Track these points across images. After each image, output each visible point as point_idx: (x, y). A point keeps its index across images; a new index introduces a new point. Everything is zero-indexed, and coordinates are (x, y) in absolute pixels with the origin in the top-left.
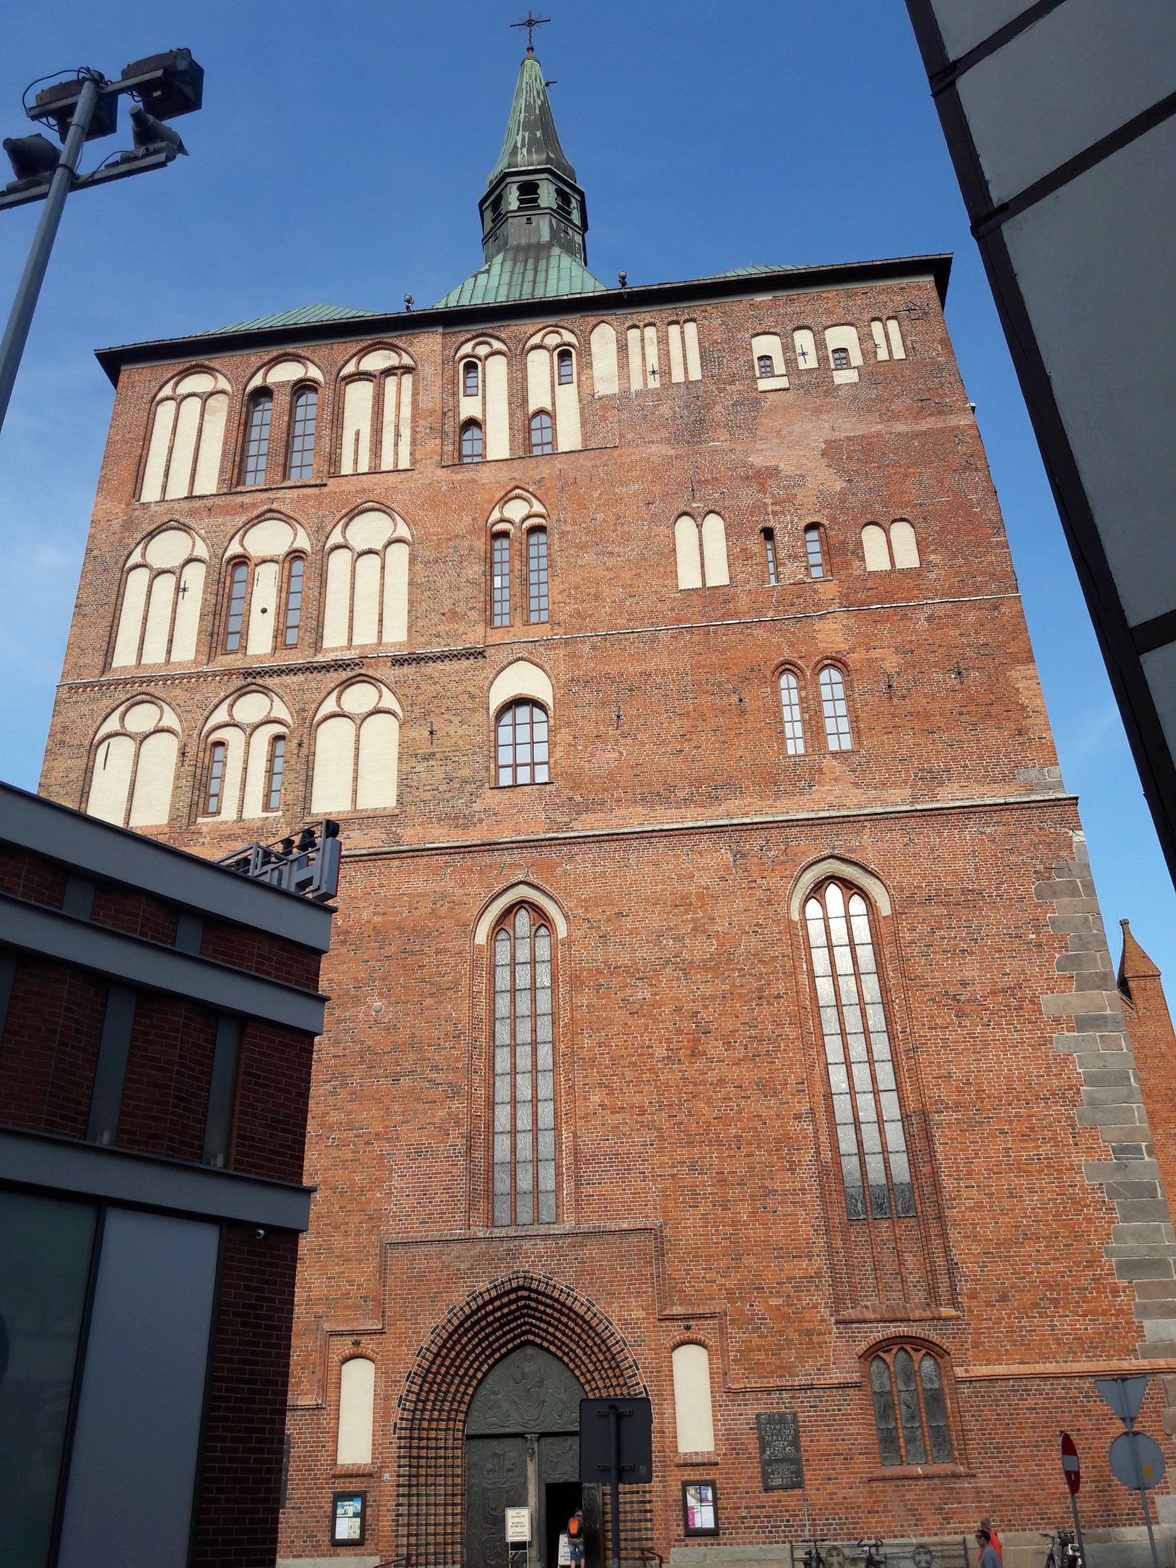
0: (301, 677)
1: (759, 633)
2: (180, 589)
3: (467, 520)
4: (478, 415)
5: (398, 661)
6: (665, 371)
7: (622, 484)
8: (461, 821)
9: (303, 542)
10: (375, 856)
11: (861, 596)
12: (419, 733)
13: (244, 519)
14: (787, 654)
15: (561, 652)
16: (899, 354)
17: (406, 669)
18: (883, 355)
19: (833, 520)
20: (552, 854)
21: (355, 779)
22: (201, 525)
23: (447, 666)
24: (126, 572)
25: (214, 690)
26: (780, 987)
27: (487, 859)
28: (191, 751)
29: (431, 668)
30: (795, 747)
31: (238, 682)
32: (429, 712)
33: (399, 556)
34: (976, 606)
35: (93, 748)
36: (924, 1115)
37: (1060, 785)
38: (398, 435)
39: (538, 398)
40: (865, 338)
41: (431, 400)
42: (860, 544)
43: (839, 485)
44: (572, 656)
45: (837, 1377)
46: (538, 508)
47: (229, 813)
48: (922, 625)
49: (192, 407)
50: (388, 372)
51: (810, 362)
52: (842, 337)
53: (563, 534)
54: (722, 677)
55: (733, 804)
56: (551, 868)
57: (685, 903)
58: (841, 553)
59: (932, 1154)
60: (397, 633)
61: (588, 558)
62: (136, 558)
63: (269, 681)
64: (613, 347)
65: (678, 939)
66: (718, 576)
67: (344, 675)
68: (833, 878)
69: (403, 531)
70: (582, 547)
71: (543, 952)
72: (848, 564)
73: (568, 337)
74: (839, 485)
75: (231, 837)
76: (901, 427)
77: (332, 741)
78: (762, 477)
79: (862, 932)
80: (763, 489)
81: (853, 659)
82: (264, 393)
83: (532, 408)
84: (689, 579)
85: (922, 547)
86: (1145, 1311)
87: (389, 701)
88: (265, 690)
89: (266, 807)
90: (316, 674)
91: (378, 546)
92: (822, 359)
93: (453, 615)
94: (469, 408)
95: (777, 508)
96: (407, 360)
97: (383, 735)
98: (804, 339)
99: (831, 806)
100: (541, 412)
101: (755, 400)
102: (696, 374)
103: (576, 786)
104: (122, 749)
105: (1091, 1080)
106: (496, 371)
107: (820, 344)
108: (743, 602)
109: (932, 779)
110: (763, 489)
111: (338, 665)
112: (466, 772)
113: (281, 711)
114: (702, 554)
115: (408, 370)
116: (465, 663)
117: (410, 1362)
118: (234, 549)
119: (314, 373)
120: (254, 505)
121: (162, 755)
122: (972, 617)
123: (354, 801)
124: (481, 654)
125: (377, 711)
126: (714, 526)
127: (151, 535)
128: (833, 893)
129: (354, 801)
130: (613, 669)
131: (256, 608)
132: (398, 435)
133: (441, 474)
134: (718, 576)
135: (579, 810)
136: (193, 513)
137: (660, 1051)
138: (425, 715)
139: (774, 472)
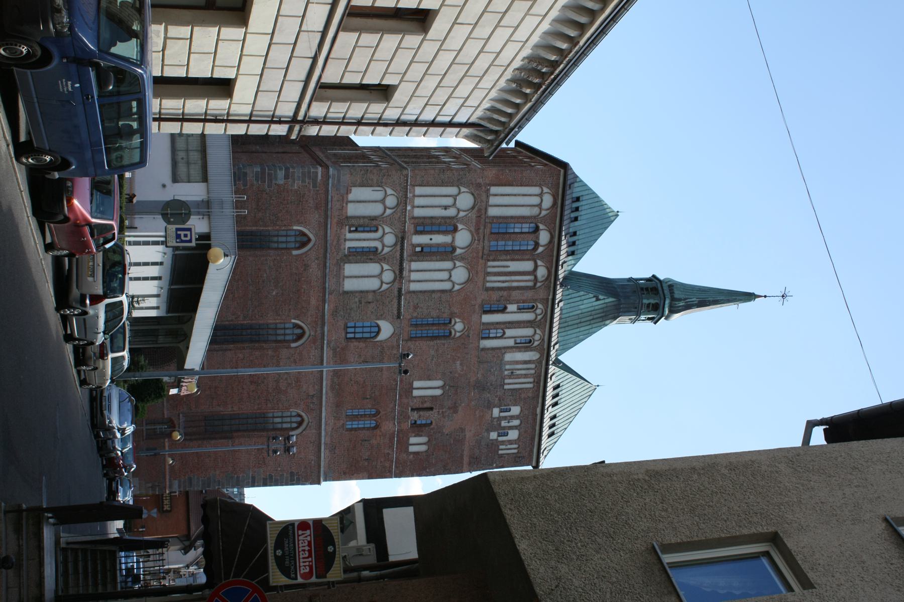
0: (398, 257)
1: (392, 405)
3: (456, 311)
4: (508, 310)
5: (400, 290)
6: (512, 375)
7: (461, 364)
9: (458, 251)
10: (324, 288)
11: (401, 435)
12: (370, 297)
14: (382, 413)
15: (395, 343)
16: (500, 452)
17: (396, 293)
18: (501, 447)
19: (433, 429)
21: (356, 277)
22: (473, 215)
23: (396, 305)
26: (269, 405)
27: (319, 323)
28: (374, 223)
29: (395, 301)
30: (349, 412)
32: (377, 301)
33: (447, 286)
34: (391, 467)
36: (231, 438)
37: (325, 480)
38: (503, 282)
39: (509, 332)
40: (510, 442)
42: (421, 436)
43: (446, 431)
45: (165, 412)
46: (458, 334)
47: (349, 236)
48: (387, 451)
49: (536, 200)
50: (536, 277)
51: (504, 424)
52: (513, 435)
53: (444, 344)
54: (377, 393)
55: (330, 394)
56: (314, 343)
58: (418, 429)
59: (221, 438)
60: (414, 287)
61: (432, 352)
62: (463, 189)
63: (398, 247)
64: (528, 359)
65: (286, 379)
66: (416, 393)
67: (397, 272)
68: (303, 421)
69: (457, 287)
70: (437, 350)
71: (288, 338)
72: (413, 432)
73: (536, 343)
74: (446, 431)
77: (373, 268)
78: (454, 408)
79: (285, 426)
80: (449, 408)
81: (378, 432)
83: (506, 331)
84: (416, 384)
85: (416, 454)
86: (180, 482)
87: (385, 287)
88: (395, 244)
90: (398, 263)
91: (453, 279)
92: (504, 428)
93: (416, 307)
94: (512, 307)
96: (539, 284)
97: (373, 284)
98: (516, 422)
99: (326, 422)
100: (504, 333)
101: (490, 406)
102: (506, 387)
103: (343, 349)
104: (379, 195)
105: (238, 477)
106: (528, 316)
107: (511, 428)
108: (405, 401)
109: (332, 448)
110: (449, 408)
111: (401, 270)
113: (386, 250)
114: (426, 388)
115: (535, 284)
116: (396, 312)
118: (460, 226)
119: (541, 249)
120: (478, 234)
121: (375, 210)
122: (387, 465)
123: (347, 277)
124: (399, 317)
125: (382, 282)
126: (438, 392)
128: (299, 419)
129: (347, 277)
131: (432, 236)
132: (503, 282)
133: (479, 301)
134: (416, 393)
135: (334, 350)
136: (479, 210)
138: (377, 301)
139: (456, 412)
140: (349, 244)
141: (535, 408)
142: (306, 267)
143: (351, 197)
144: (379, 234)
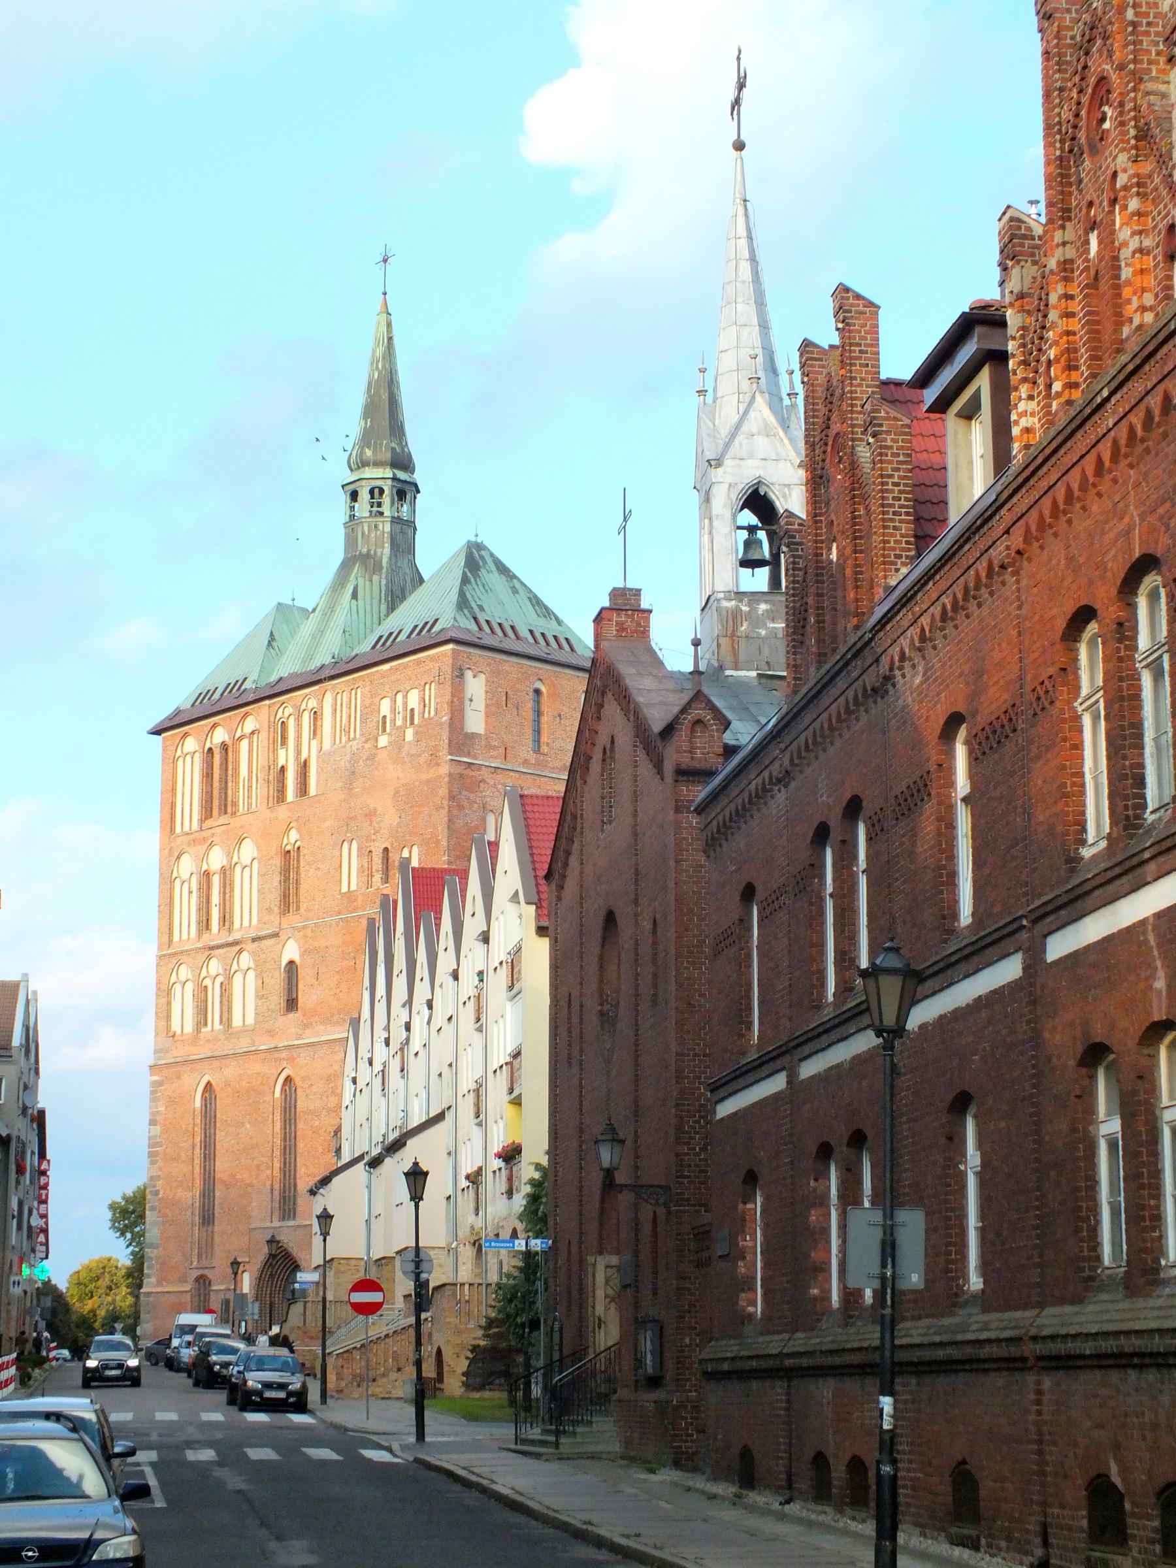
2: (190, 892)
5: (254, 940)
8: (271, 1033)
13: (205, 847)
20: (294, 1053)
24: (172, 882)
25: (202, 957)
27: (276, 1055)
31: (207, 953)
35: (169, 990)
41: (261, 759)
44: (305, 936)
50: (253, 733)
57: (329, 1080)
63: (216, 952)
67: (238, 948)
75: (208, 1041)
76: (424, 777)
82: (210, 749)
84: (344, 889)
89: (221, 1022)
92: (405, 719)
95: (374, 837)
108: (360, 899)
111: (236, 943)
112: (272, 1006)
117: (256, 1274)
118: (205, 867)
127: (178, 858)
130: (316, 944)
135: (307, 1026)
137: (320, 1150)
140: (217, 1026)
141: (383, 675)
142: (227, 1084)
143: (179, 1032)
144: (208, 982)
